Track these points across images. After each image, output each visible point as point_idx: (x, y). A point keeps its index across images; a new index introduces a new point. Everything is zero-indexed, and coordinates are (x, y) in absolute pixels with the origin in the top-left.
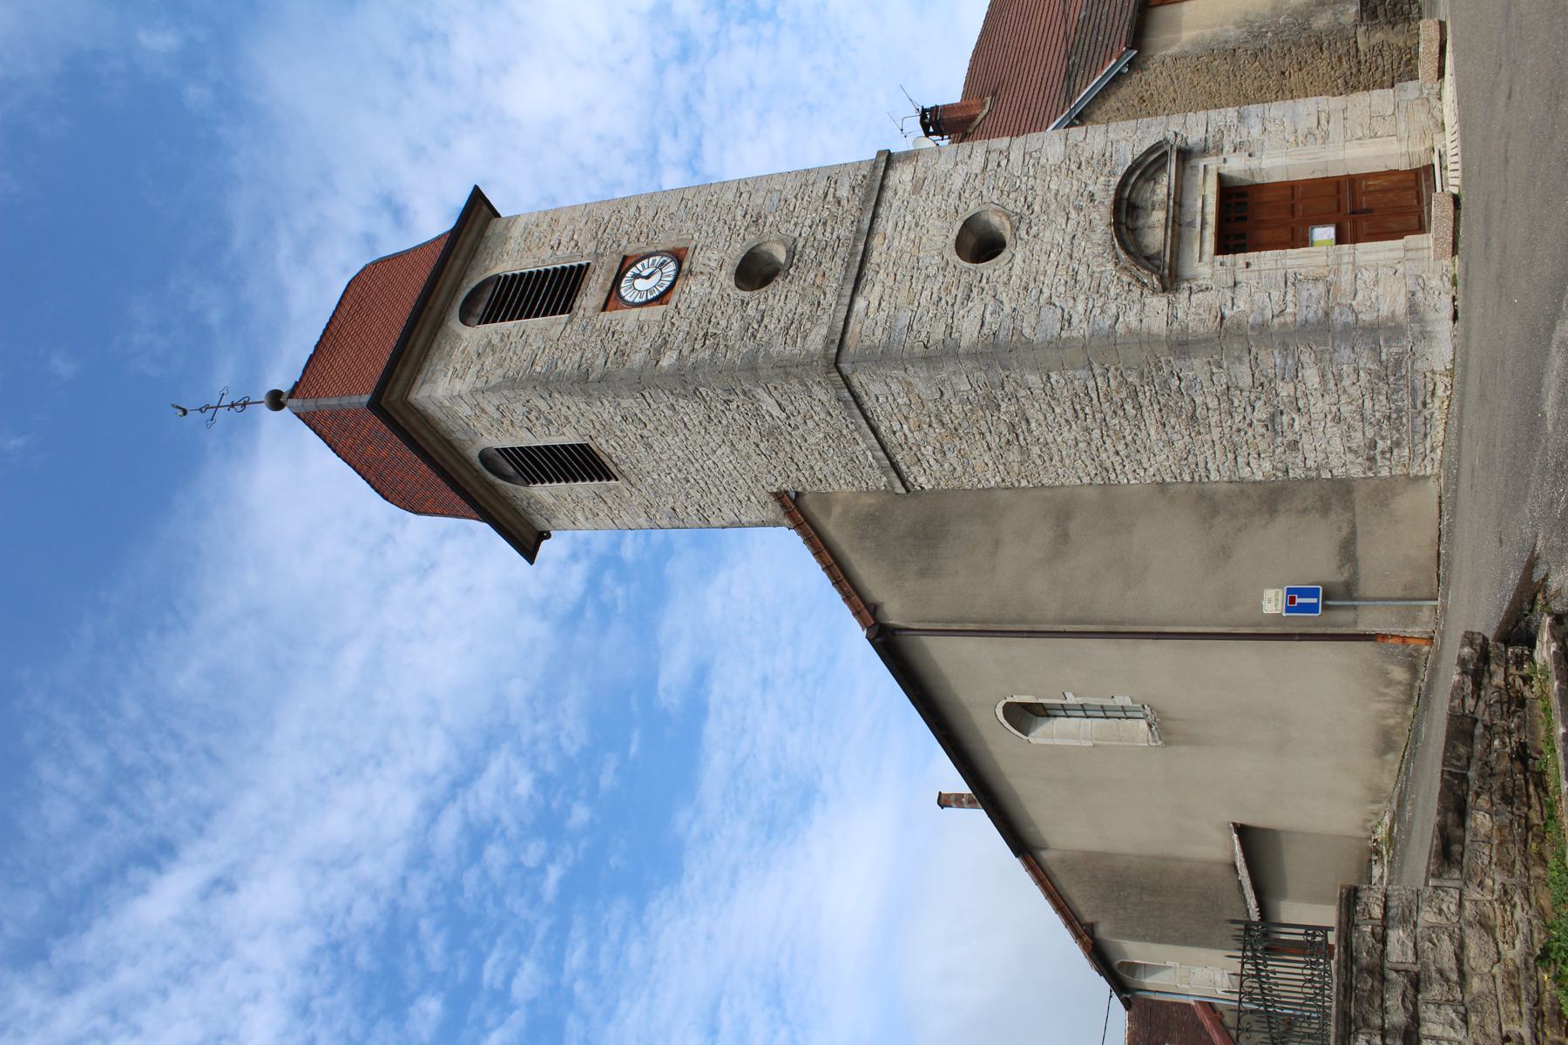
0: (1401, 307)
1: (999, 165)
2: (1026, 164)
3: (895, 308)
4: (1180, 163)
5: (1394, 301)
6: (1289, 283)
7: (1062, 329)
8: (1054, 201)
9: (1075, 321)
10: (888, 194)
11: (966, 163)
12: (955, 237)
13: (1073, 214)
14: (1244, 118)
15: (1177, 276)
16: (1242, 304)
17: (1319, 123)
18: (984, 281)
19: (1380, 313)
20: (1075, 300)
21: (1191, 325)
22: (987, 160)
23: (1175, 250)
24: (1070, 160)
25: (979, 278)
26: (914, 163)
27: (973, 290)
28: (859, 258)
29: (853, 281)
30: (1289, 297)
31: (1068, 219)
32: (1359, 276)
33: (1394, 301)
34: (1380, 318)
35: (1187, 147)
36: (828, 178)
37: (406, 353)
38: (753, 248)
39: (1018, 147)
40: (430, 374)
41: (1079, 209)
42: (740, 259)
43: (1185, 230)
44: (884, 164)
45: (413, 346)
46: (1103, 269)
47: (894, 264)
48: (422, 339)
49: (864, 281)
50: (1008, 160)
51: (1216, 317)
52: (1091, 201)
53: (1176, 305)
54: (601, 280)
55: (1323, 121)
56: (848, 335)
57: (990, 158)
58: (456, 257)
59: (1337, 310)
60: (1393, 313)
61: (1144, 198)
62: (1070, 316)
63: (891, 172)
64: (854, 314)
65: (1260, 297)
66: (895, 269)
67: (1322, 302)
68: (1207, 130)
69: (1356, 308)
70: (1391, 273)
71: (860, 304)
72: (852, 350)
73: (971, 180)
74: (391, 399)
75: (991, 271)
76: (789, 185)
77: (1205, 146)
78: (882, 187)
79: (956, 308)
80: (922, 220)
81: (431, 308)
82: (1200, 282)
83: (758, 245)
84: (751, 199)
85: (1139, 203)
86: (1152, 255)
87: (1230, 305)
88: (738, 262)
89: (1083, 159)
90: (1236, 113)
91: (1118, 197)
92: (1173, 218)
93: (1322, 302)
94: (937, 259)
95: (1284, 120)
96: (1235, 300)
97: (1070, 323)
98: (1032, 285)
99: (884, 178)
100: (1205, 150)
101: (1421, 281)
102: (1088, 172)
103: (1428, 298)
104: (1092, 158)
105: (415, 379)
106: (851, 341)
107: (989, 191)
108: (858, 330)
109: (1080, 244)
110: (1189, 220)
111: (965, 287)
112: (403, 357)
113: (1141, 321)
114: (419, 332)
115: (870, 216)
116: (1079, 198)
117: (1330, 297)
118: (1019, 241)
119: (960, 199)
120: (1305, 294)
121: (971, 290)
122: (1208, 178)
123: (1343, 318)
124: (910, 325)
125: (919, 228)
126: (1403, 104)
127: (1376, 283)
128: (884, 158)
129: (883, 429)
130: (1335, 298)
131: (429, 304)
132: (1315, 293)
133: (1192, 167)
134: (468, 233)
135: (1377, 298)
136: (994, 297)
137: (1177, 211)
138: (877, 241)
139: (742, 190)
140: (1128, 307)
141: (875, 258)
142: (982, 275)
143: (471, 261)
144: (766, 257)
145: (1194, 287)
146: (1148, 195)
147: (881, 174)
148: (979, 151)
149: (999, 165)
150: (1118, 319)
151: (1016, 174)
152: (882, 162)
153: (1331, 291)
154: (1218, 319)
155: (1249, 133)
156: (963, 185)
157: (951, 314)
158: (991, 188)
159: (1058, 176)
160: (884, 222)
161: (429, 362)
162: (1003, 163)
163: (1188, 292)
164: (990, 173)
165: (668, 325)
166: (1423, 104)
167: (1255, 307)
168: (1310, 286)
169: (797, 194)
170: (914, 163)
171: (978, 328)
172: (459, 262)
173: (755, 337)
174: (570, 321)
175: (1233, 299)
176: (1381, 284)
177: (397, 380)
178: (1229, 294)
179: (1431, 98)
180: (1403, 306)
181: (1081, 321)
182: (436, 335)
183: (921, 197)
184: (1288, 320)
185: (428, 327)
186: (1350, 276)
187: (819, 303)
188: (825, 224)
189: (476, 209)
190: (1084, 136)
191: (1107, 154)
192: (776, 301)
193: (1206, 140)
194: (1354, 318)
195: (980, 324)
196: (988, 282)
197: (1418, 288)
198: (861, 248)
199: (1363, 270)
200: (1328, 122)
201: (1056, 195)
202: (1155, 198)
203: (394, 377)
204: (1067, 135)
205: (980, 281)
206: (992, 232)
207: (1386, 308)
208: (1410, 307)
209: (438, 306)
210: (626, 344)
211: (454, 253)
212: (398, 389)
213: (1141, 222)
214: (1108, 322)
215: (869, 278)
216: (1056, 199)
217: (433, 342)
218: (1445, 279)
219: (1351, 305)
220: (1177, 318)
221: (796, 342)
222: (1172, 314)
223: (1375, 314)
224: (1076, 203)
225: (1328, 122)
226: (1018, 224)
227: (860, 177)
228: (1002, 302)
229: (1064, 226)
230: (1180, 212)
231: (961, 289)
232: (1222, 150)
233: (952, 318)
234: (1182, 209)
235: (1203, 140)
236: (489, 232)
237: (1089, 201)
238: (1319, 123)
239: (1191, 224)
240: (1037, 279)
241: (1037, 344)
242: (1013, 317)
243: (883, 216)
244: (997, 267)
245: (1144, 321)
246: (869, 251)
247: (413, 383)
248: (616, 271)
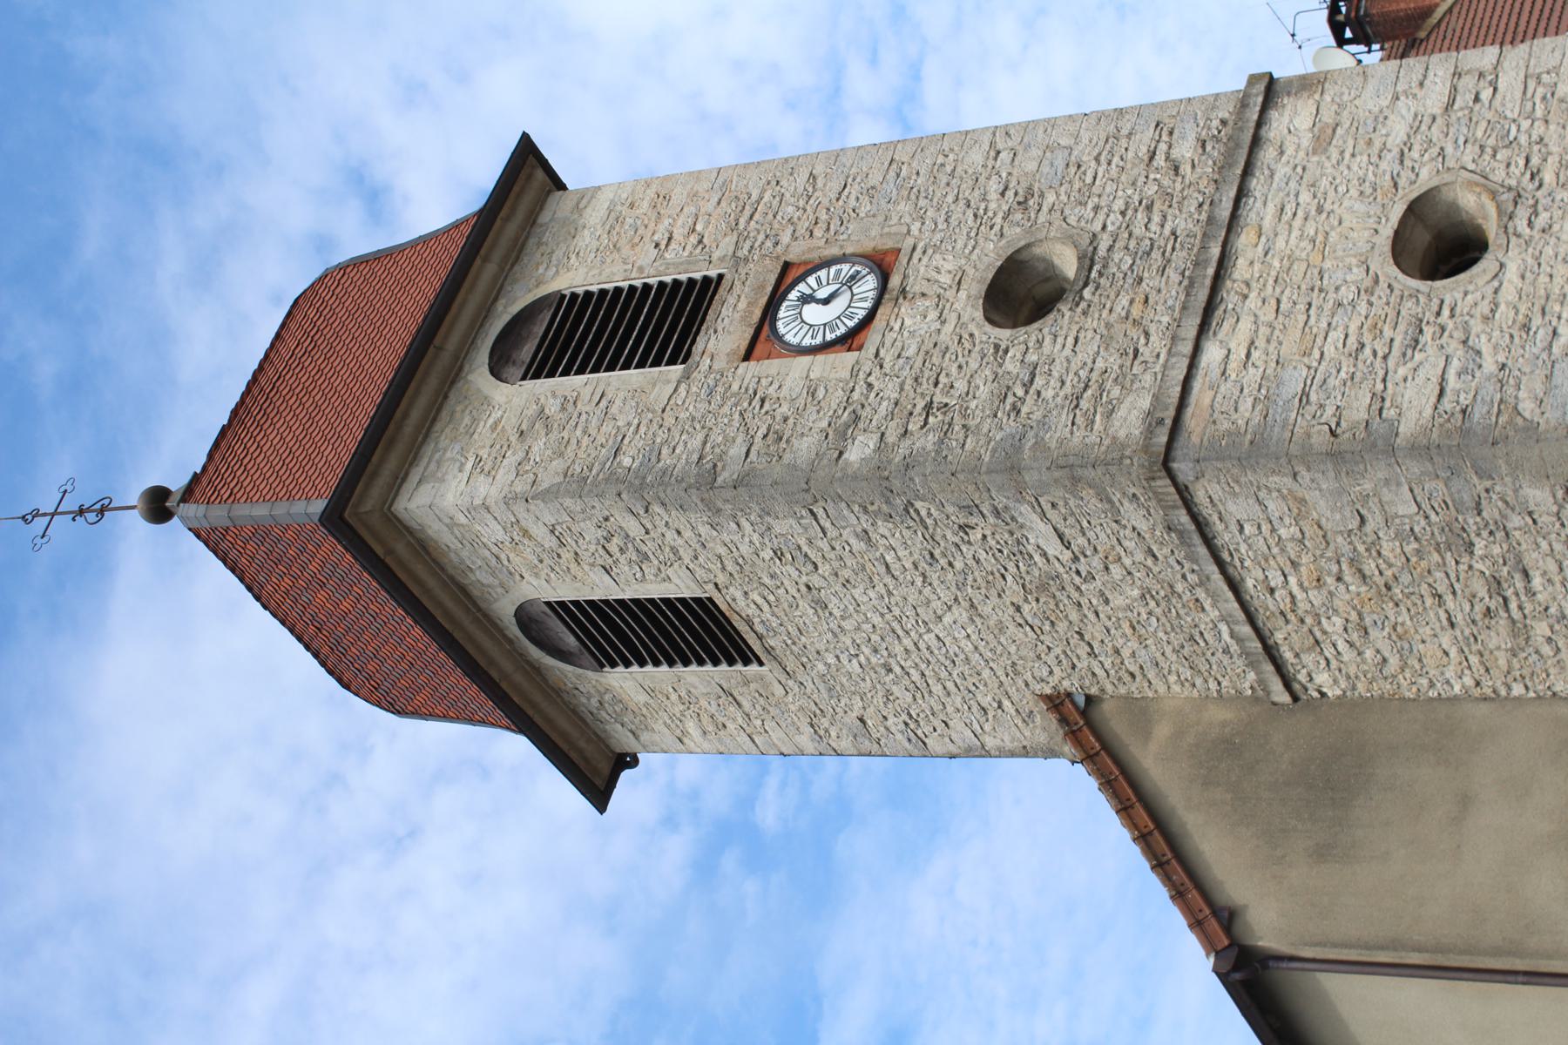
1: (1477, 99)
2: (1529, 95)
3: (1278, 363)
10: (1267, 154)
11: (1415, 96)
18: (1446, 312)
22: (1454, 89)
25: (1435, 308)
26: (1317, 96)
27: (1425, 328)
28: (1211, 271)
29: (1200, 311)
36: (1157, 125)
37: (392, 426)
38: (1018, 251)
39: (1514, 64)
40: (433, 466)
42: (994, 271)
44: (1260, 99)
45: (406, 415)
47: (1276, 281)
48: (422, 401)
49: (1219, 312)
50: (1495, 89)
54: (742, 305)
56: (1189, 411)
57: (1460, 88)
58: (486, 260)
63: (1273, 114)
64: (1201, 372)
66: (1278, 290)
71: (1212, 354)
72: (1195, 439)
73: (1424, 127)
74: (363, 509)
75: (1459, 296)
76: (1085, 136)
78: (1256, 141)
79: (1391, 362)
80: (1329, 201)
81: (440, 349)
83: (1028, 246)
84: (1016, 163)
88: (990, 276)
94: (1357, 273)
98: (1537, 321)
99: (1260, 124)
105: (407, 474)
106: (1193, 421)
108: (1207, 401)
111: (1410, 324)
112: (388, 433)
114: (417, 392)
115: (1233, 193)
118: (1513, 240)
119: (1402, 162)
121: (1421, 331)
124: (1305, 394)
125: (1324, 215)
128: (1261, 87)
129: (1250, 583)
131: (437, 341)
134: (507, 219)
136: (1465, 342)
138: (1244, 241)
139: (1000, 146)
141: (1241, 270)
142: (1442, 302)
143: (513, 266)
144: (1041, 266)
147: (1255, 117)
148: (1440, 73)
149: (1477, 99)
151: (1509, 115)
152: (1257, 95)
156: (1409, 137)
157: (1381, 373)
161: (432, 445)
162: (1486, 95)
164: (1460, 114)
165: (861, 388)
169: (1100, 154)
170: (1317, 96)
171: (1433, 399)
172: (491, 269)
173: (1019, 412)
174: (686, 376)
177: (375, 474)
182: (446, 397)
183: (1328, 158)
185: (433, 382)
187: (1136, 352)
188: (1149, 208)
189: (523, 175)
192: (1058, 346)
195: (1437, 392)
196: (1452, 316)
198: (1215, 251)
203: (370, 468)
205: (1438, 314)
206: (1462, 222)
210: (786, 420)
211: (482, 252)
212: (376, 491)
215: (1230, 306)
217: (439, 410)
221: (1093, 422)
226: (1511, 208)
227: (1216, 123)
228: (1479, 353)
231: (1401, 327)
233: (1384, 380)
236: (545, 217)
240: (1547, 310)
241: (1547, 431)
242: (1500, 381)
243: (1257, 194)
244: (1471, 288)
246: (1230, 259)
247: (404, 480)
248: (769, 289)
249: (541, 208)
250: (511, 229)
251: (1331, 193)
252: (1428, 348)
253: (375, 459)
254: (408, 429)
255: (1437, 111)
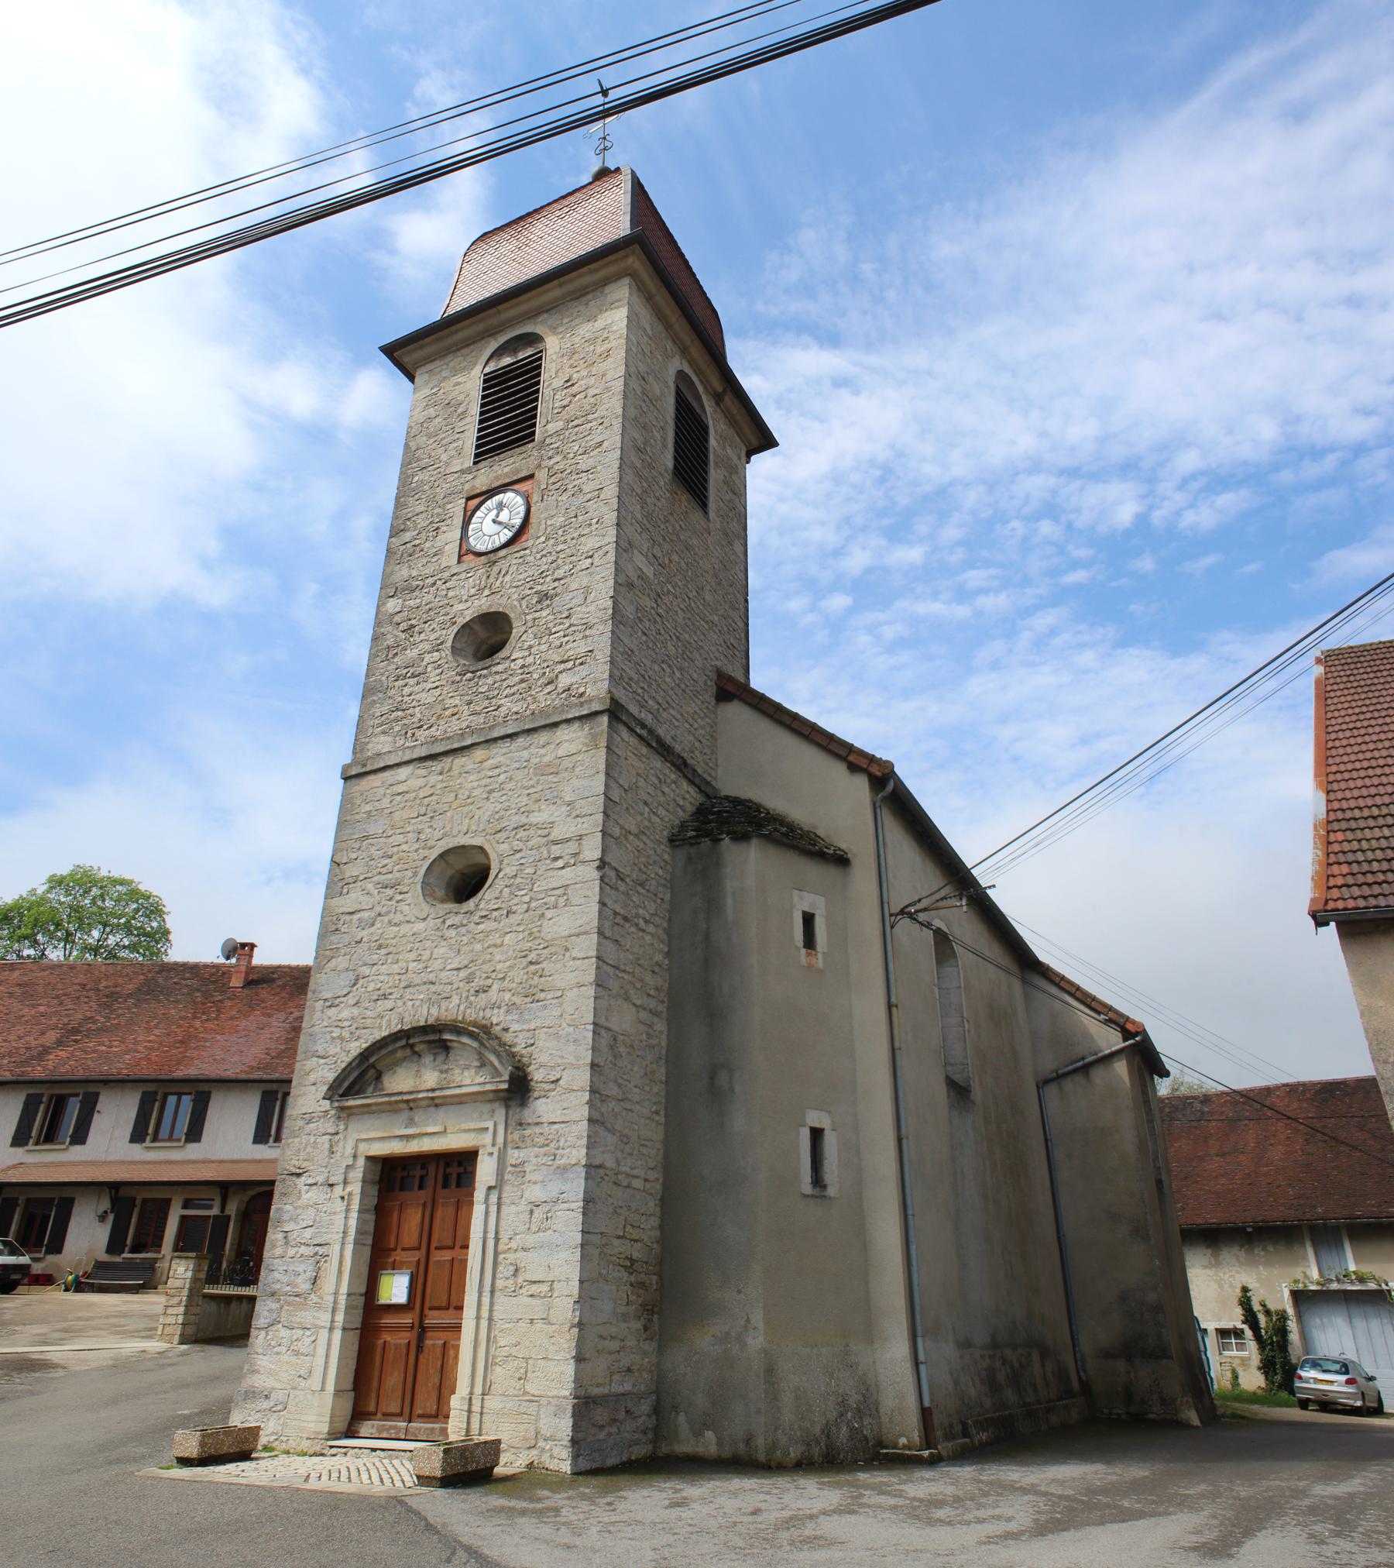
0: (259, 1381)
1: (556, 859)
2: (550, 893)
4: (491, 1095)
5: (270, 1373)
6: (317, 1248)
7: (325, 1000)
8: (486, 945)
9: (332, 1012)
10: (543, 737)
12: (462, 843)
13: (463, 974)
14: (562, 1174)
15: (349, 1116)
16: (310, 1196)
17: (535, 1282)
19: (261, 1357)
20: (354, 1005)
21: (297, 1140)
22: (568, 840)
23: (374, 1108)
24: (544, 948)
26: (584, 749)
29: (429, 753)
30: (303, 1250)
31: (458, 969)
32: (308, 1333)
33: (270, 1373)
34: (256, 1356)
35: (531, 1099)
36: (590, 651)
37: (446, 331)
40: (437, 370)
41: (469, 980)
43: (405, 1114)
44: (585, 712)
45: (456, 332)
46: (384, 1028)
50: (563, 868)
51: (299, 1168)
52: (476, 991)
53: (322, 1120)
54: (506, 470)
55: (534, 1289)
58: (561, 285)
59: (275, 1306)
60: (258, 1372)
61: (458, 1058)
62: (338, 1005)
65: (308, 1216)
67: (288, 1288)
68: (555, 1123)
69: (273, 1328)
70: (302, 1372)
71: (404, 772)
77: (529, 1124)
81: (499, 312)
82: (341, 1144)
85: (451, 1056)
86: (382, 1083)
87: (309, 1182)
89: (544, 965)
90: (573, 1162)
91: (441, 1027)
92: (415, 1100)
93: (288, 1288)
94: (438, 834)
95: (550, 1232)
96: (314, 1187)
97: (330, 1007)
98: (383, 951)
99: (568, 721)
100: (521, 1124)
101: (279, 1407)
102: (518, 975)
103: (259, 1415)
104: (541, 976)
105: (435, 360)
107: (518, 860)
108: (375, 785)
109: (421, 992)
110: (416, 1119)
113: (314, 1084)
114: (470, 325)
116: (484, 975)
117: (292, 1298)
118: (441, 920)
120: (300, 1268)
122: (472, 1135)
123: (266, 1313)
124: (367, 837)
126: (532, 1409)
127: (297, 1353)
129: (685, 784)
130: (289, 1304)
131: (501, 307)
132: (300, 1280)
133: (493, 1111)
134: (591, 272)
135: (278, 1353)
136: (379, 915)
137: (424, 1103)
140: (333, 1066)
141: (459, 761)
143: (571, 300)
145: (337, 1137)
146: (462, 1062)
147: (570, 716)
148: (585, 825)
150: (323, 1057)
151: (536, 886)
153: (297, 1299)
154: (298, 1171)
155: (535, 1183)
157: (370, 875)
158: (522, 861)
159: (523, 939)
160: (504, 750)
162: (560, 863)
163: (332, 1131)
166: (525, 1439)
167: (299, 1211)
168: (308, 1274)
169: (575, 625)
173: (397, 680)
175: (316, 1184)
176: (293, 1359)
177: (421, 347)
178: (321, 1179)
179: (534, 1452)
180: (262, 1384)
181: (330, 1018)
182: (483, 339)
184: (277, 1250)
185: (481, 327)
186: (308, 1323)
188: (522, 681)
189: (622, 253)
190: (580, 955)
191: (542, 995)
192: (433, 680)
193: (537, 1124)
194: (262, 1326)
197: (272, 1404)
198: (469, 742)
199: (313, 1338)
200: (531, 1296)
201: (495, 945)
202: (457, 1071)
203: (421, 343)
204: (586, 933)
205: (400, 893)
207: (264, 1363)
208: (253, 1392)
209: (504, 316)
210: (422, 550)
211: (562, 279)
213: (427, 1059)
214: (320, 1049)
215: (433, 768)
216: (488, 948)
217: (474, 343)
218: (272, 1438)
219: (279, 1322)
220: (307, 1123)
222: (313, 1118)
223: (260, 1351)
224: (478, 973)
225: (531, 1296)
226: (462, 911)
227: (582, 690)
228: (373, 925)
229: (448, 967)
230: (429, 1106)
232: (517, 1148)
233: (366, 878)
234: (433, 1109)
235: (539, 1120)
236: (607, 289)
237: (477, 989)
238: (535, 1282)
239: (411, 1122)
242: (349, 944)
244: (412, 906)
245: (313, 1087)
247: (431, 361)
248: (515, 478)
249: (616, 280)
250: (587, 280)
251: (500, 794)
252: (381, 895)
253: (427, 340)
254: (450, 340)
255: (551, 838)
